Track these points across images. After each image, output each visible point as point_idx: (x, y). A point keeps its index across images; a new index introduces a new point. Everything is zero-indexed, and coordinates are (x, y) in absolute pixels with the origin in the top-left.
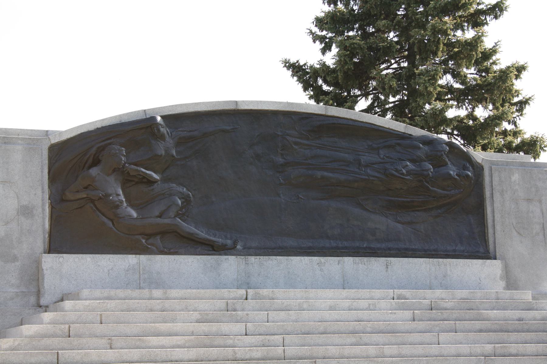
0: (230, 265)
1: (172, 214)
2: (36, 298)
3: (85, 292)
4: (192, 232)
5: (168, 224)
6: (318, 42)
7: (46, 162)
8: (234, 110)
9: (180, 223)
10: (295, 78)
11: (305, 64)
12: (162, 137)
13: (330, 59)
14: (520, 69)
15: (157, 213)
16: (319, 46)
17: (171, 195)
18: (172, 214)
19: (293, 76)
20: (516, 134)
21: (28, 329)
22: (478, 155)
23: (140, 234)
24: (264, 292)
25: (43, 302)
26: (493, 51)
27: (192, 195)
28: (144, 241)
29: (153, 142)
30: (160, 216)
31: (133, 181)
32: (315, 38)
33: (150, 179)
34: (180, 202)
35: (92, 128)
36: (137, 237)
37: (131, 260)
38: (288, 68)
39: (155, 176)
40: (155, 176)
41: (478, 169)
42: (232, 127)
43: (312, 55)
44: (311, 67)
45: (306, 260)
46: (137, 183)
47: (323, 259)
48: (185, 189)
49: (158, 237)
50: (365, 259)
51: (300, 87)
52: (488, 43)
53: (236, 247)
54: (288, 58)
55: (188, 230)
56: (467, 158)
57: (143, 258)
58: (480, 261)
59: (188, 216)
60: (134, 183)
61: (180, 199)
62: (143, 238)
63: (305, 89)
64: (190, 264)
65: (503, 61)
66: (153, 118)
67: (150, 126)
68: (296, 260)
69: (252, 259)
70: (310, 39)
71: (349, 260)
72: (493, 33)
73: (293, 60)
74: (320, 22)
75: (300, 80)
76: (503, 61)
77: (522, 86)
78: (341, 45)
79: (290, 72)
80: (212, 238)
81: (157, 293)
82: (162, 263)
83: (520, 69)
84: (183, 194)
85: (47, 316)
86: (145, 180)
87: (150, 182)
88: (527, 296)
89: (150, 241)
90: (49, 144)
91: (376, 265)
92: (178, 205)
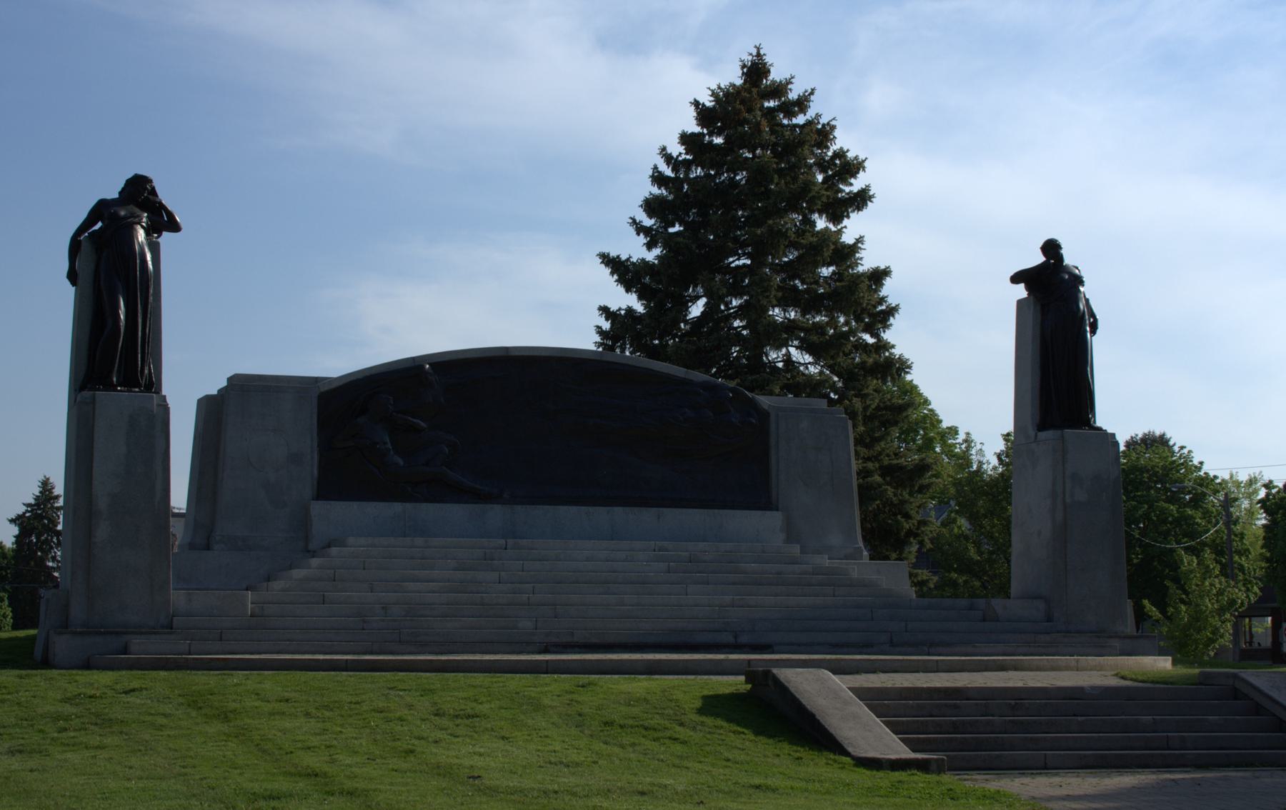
0: (496, 514)
2: (304, 543)
3: (351, 540)
6: (642, 235)
7: (315, 410)
10: (616, 277)
11: (628, 260)
13: (652, 256)
14: (879, 276)
16: (642, 239)
19: (612, 274)
20: (883, 346)
21: (298, 573)
22: (764, 401)
24: (524, 542)
25: (311, 547)
26: (854, 248)
32: (640, 229)
35: (360, 377)
37: (398, 507)
38: (607, 265)
39: (422, 424)
40: (422, 424)
41: (764, 415)
43: (636, 249)
44: (633, 264)
45: (573, 509)
47: (591, 509)
50: (636, 509)
51: (621, 289)
52: (848, 238)
54: (606, 250)
56: (753, 405)
57: (409, 506)
58: (759, 513)
63: (628, 290)
64: (455, 512)
65: (868, 261)
66: (423, 367)
68: (563, 509)
69: (518, 508)
70: (632, 231)
71: (618, 510)
72: (853, 227)
73: (613, 254)
74: (651, 206)
75: (621, 281)
76: (868, 261)
77: (890, 290)
78: (670, 243)
79: (608, 271)
81: (419, 541)
82: (429, 511)
83: (879, 276)
85: (315, 562)
88: (796, 549)
91: (646, 517)
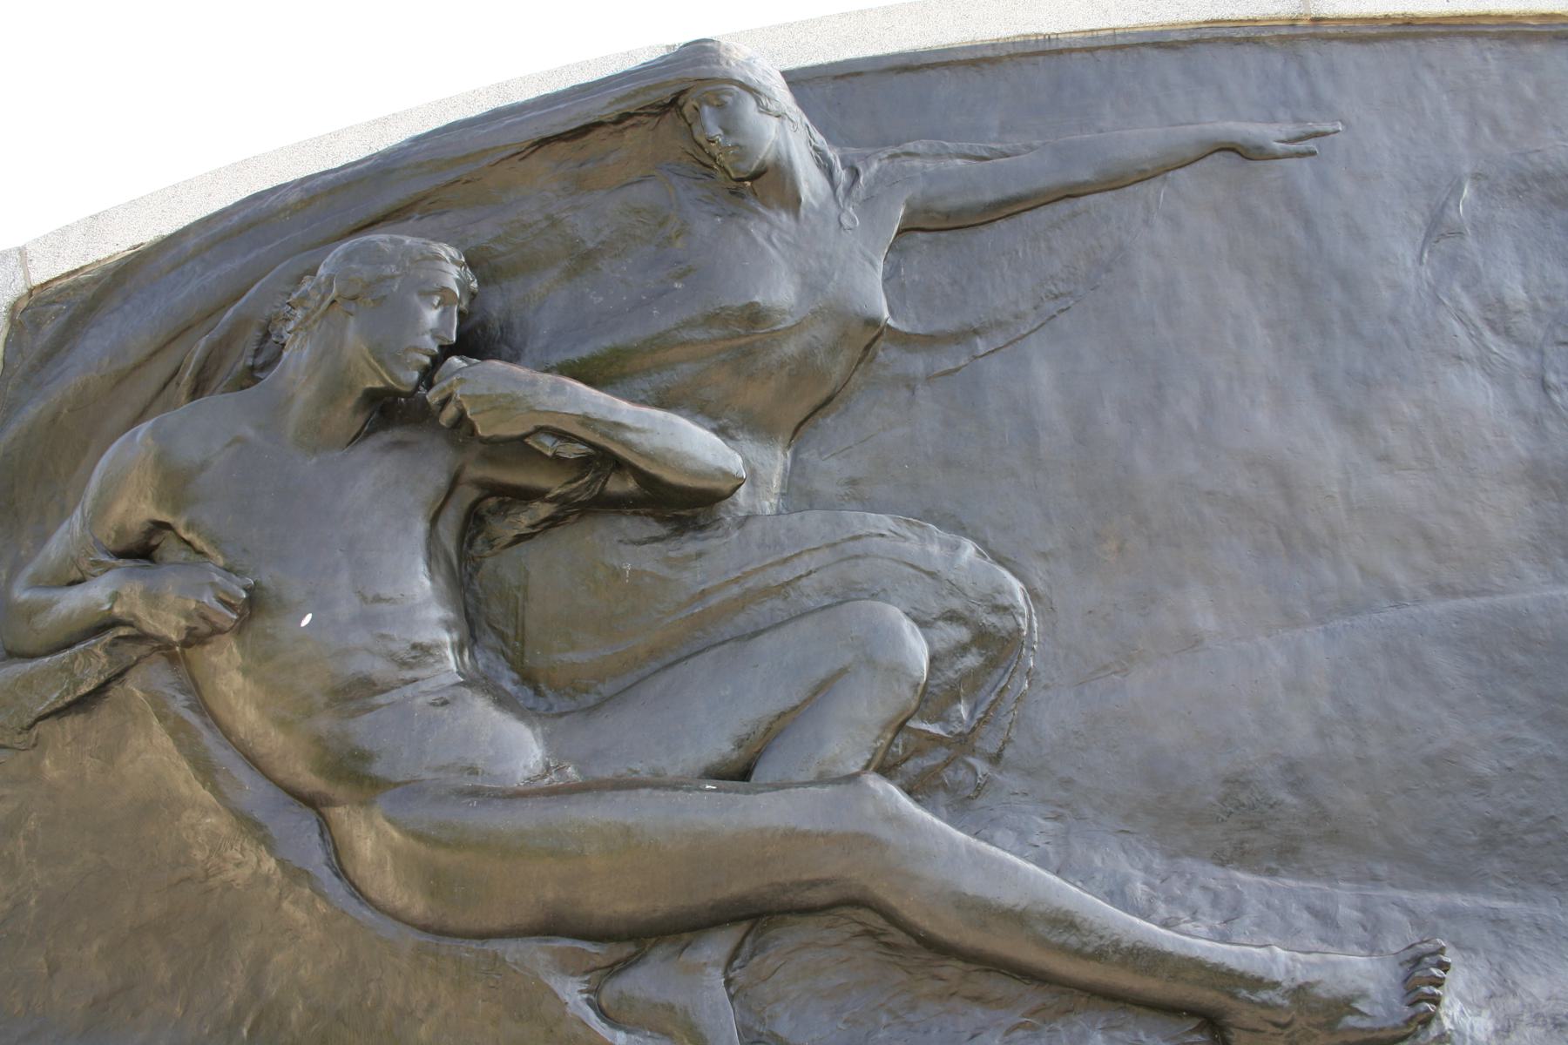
1: (848, 737)
4: (1009, 898)
5: (790, 835)
8: (1293, 22)
9: (896, 819)
12: (766, 183)
15: (720, 747)
17: (847, 594)
18: (848, 737)
23: (551, 927)
27: (1033, 594)
28: (572, 992)
29: (704, 225)
30: (739, 773)
31: (526, 495)
33: (669, 476)
34: (917, 649)
36: (511, 949)
42: (1292, 129)
46: (570, 511)
48: (969, 549)
49: (715, 948)
53: (1427, 1020)
55: (972, 884)
59: (995, 759)
60: (544, 510)
61: (923, 624)
62: (567, 967)
67: (673, 104)
80: (1197, 942)
84: (956, 589)
86: (619, 485)
87: (685, 506)
89: (645, 982)
90: (18, 288)
92: (897, 670)
